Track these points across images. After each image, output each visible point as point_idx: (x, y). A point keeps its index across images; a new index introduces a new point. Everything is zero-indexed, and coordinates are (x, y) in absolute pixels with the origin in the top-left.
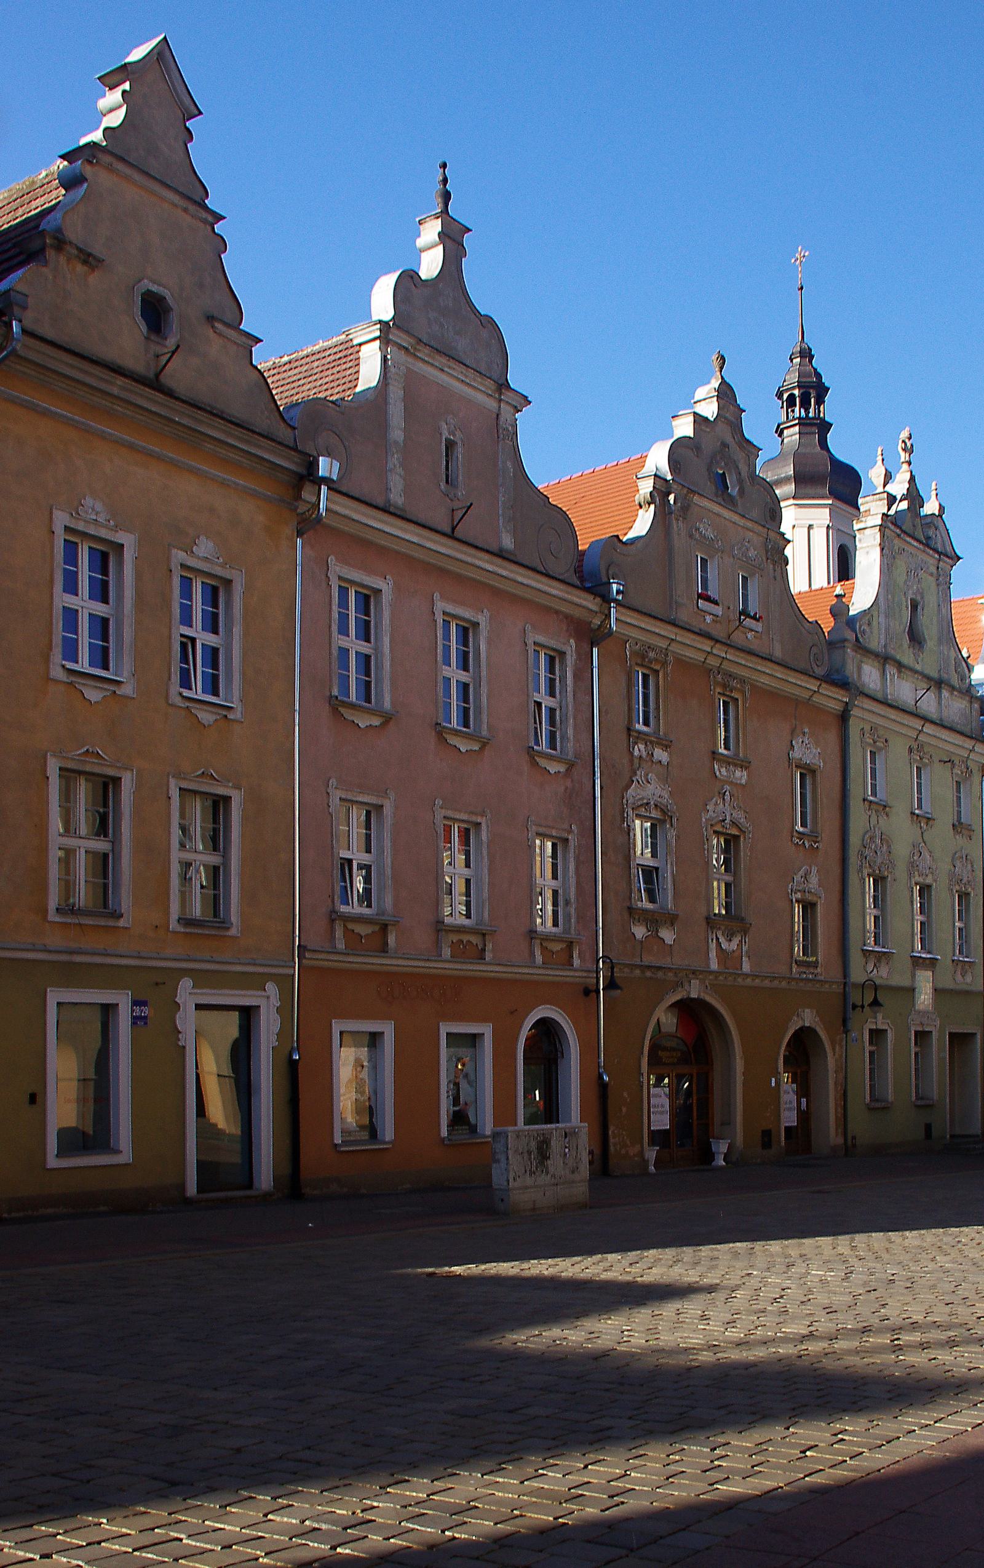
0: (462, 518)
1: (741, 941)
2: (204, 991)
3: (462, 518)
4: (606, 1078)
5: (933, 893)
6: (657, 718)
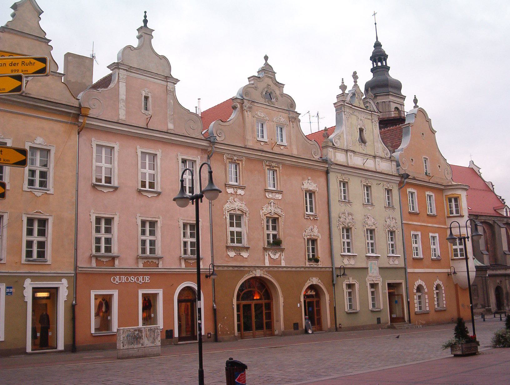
0: (149, 120)
1: (280, 255)
2: (36, 283)
3: (149, 120)
4: (215, 306)
5: (376, 233)
6: (240, 179)
